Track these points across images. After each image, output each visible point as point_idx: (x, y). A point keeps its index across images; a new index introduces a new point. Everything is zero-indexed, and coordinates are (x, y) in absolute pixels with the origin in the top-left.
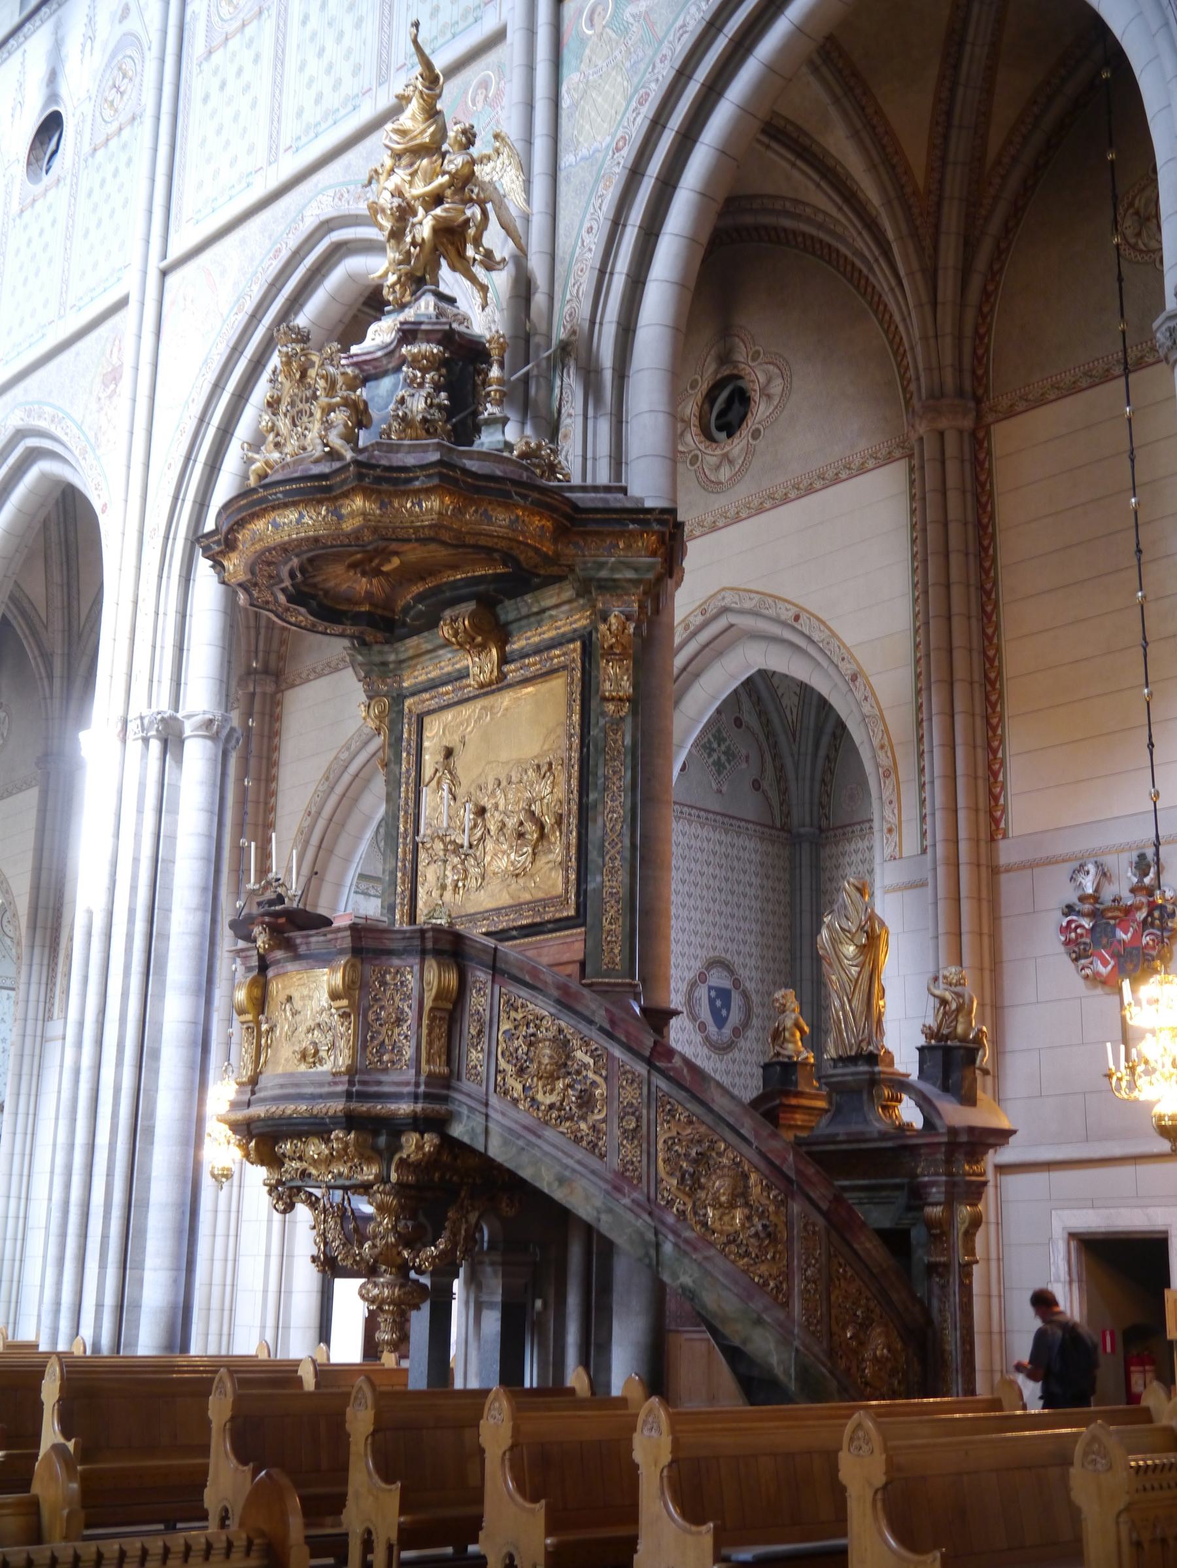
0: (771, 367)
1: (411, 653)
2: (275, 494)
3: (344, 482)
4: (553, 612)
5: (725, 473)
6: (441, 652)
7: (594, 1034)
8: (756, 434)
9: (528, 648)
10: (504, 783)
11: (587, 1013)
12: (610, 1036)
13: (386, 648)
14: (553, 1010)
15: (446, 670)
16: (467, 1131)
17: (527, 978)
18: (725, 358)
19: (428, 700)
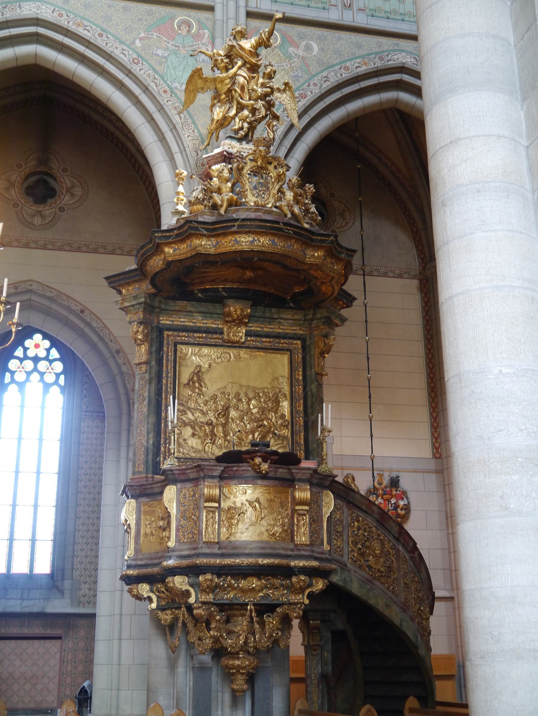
0: (75, 181)
1: (177, 308)
2: (289, 230)
3: (325, 241)
4: (282, 321)
5: (37, 221)
6: (196, 314)
7: (391, 538)
8: (62, 209)
9: (261, 332)
10: (242, 396)
11: (389, 528)
12: (398, 540)
13: (163, 301)
14: (375, 524)
15: (198, 324)
16: (341, 580)
17: (364, 508)
18: (44, 162)
19: (184, 336)
